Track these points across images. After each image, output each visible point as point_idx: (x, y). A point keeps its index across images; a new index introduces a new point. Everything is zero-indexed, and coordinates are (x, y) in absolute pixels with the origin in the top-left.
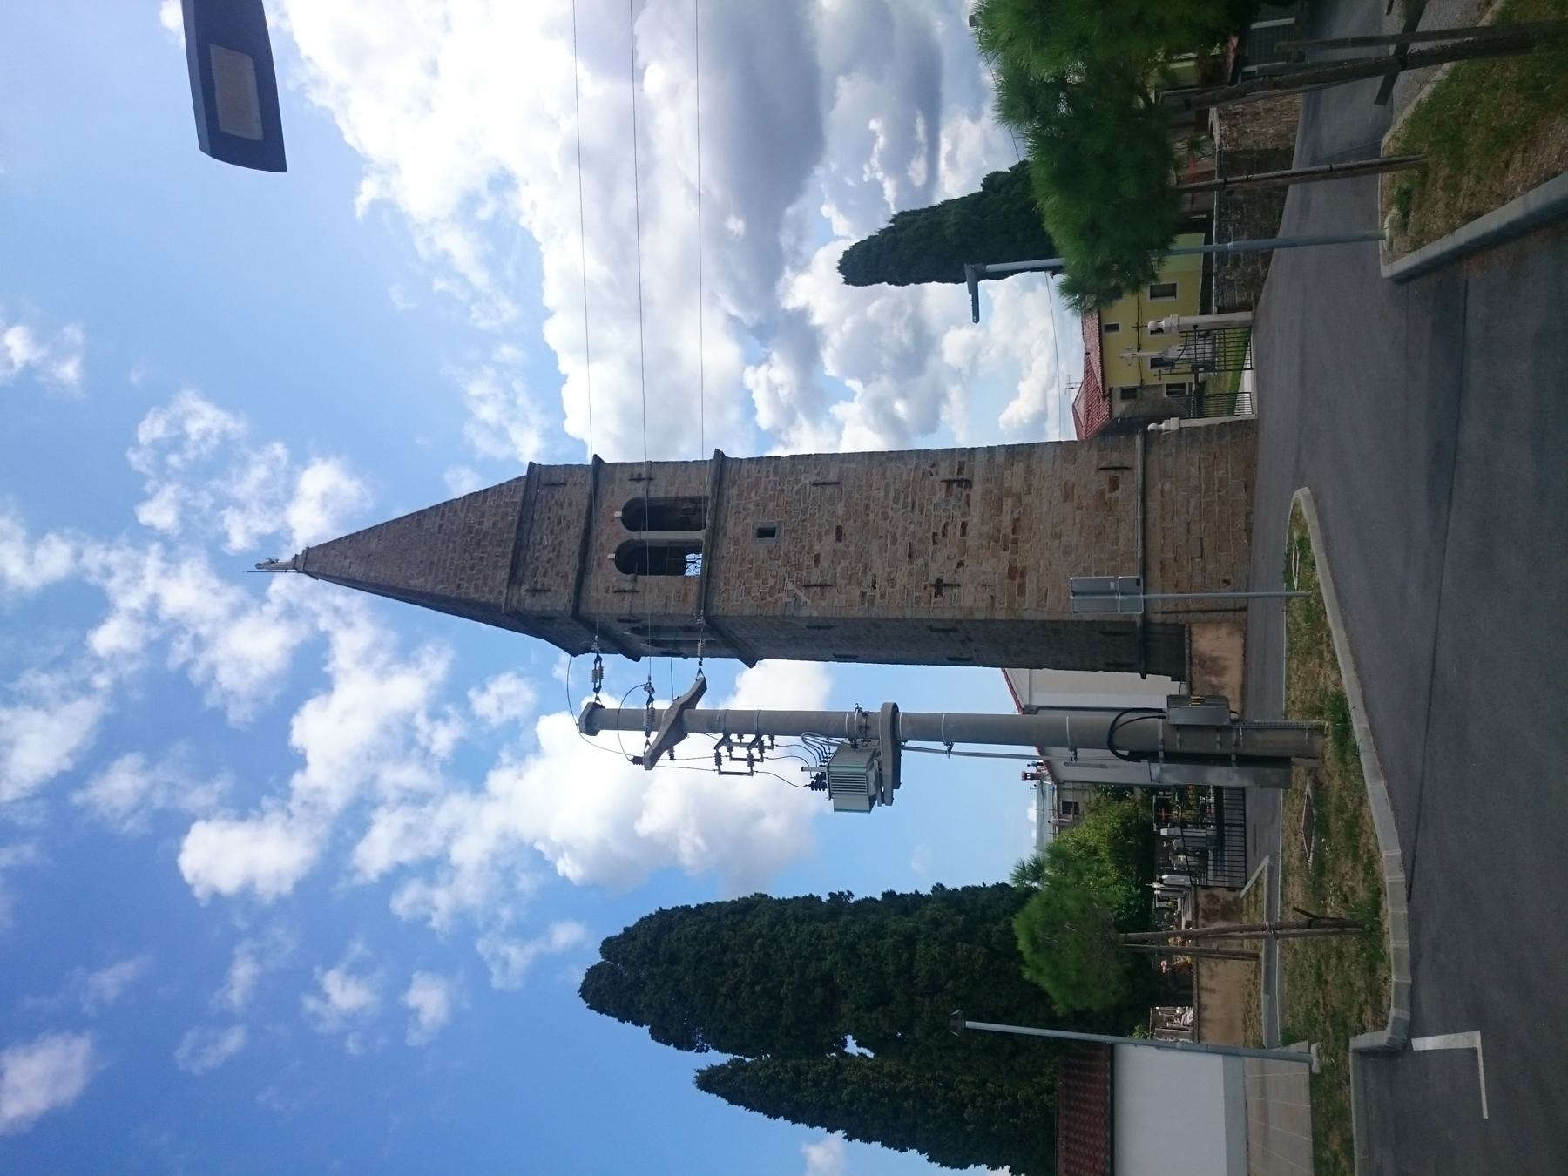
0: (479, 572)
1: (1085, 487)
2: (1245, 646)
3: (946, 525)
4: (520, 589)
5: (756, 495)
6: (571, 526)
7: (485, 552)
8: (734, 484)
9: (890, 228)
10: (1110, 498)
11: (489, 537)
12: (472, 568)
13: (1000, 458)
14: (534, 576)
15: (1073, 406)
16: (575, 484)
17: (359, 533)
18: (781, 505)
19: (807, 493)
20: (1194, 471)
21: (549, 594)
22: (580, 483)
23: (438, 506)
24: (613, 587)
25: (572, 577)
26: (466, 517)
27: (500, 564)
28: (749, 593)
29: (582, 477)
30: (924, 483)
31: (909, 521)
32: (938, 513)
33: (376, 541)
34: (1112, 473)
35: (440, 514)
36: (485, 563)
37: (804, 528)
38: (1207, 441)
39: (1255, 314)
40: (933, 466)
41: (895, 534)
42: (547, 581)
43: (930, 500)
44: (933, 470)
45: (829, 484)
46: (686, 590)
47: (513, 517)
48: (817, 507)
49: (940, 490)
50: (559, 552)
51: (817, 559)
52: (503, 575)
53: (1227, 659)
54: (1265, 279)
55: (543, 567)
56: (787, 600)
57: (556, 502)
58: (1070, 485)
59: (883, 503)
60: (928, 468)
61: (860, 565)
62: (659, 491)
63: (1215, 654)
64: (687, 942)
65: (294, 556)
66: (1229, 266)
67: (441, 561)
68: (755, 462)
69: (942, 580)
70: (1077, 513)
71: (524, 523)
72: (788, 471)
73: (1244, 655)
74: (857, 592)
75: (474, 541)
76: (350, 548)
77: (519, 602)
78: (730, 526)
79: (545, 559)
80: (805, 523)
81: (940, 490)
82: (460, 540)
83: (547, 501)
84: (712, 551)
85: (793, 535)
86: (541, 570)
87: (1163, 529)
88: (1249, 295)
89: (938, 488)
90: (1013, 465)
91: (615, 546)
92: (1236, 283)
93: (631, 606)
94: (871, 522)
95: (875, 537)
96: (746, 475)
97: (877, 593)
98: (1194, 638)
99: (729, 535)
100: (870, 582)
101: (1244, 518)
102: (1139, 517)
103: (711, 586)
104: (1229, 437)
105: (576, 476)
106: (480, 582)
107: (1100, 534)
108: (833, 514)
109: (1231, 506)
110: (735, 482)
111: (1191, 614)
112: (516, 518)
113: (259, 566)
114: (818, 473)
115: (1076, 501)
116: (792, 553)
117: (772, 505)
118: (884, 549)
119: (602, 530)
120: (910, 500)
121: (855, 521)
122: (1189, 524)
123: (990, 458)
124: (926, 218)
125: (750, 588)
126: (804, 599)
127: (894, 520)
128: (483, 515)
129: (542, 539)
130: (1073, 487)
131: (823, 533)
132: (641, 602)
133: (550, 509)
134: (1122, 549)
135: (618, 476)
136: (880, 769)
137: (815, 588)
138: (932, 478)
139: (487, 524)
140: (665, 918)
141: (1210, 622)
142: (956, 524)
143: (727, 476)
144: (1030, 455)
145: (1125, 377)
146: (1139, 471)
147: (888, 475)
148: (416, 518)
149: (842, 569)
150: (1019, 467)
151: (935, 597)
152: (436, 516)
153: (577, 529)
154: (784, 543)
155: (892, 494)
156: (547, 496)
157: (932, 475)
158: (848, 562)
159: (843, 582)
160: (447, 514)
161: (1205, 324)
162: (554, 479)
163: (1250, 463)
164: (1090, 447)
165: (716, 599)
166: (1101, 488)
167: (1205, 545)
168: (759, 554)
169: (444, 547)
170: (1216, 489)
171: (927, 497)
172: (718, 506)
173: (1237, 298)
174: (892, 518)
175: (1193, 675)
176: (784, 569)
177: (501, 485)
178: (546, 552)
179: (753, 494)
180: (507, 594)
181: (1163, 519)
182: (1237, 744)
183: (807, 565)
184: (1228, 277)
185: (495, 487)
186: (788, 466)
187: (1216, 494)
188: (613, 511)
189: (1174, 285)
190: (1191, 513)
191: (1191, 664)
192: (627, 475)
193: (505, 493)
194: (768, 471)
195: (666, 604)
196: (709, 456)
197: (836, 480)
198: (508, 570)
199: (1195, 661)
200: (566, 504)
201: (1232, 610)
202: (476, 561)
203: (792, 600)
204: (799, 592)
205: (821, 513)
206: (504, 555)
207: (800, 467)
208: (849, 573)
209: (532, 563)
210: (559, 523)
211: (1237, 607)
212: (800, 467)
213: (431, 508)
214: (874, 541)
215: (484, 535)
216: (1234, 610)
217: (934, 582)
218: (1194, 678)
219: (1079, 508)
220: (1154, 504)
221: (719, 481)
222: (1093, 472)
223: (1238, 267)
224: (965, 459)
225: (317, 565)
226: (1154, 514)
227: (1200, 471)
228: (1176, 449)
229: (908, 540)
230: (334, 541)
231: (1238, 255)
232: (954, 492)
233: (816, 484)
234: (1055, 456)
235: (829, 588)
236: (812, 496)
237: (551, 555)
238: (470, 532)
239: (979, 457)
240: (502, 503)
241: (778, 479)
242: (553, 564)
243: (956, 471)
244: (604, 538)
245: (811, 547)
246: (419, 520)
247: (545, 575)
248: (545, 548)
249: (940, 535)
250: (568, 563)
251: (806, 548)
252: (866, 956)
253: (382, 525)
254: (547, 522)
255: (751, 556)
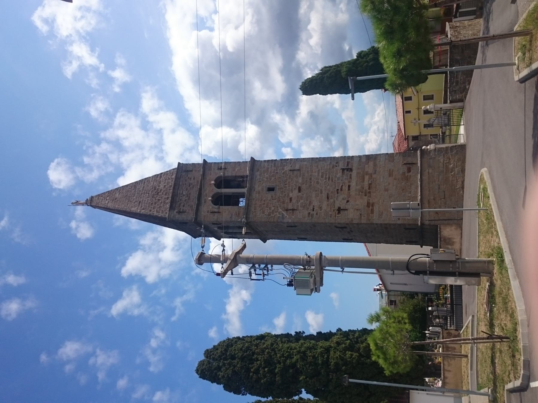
3: (342, 186)
5: (267, 175)
8: (258, 170)
9: (320, 73)
10: (408, 175)
13: (364, 160)
14: (179, 206)
15: (393, 143)
16: (196, 171)
18: (277, 178)
21: (186, 213)
24: (210, 211)
25: (195, 207)
26: (153, 184)
28: (264, 213)
31: (327, 185)
32: (339, 181)
34: (408, 166)
37: (285, 187)
40: (337, 163)
42: (185, 208)
43: (336, 176)
44: (337, 165)
45: (296, 170)
46: (239, 212)
47: (172, 183)
49: (340, 172)
50: (189, 197)
52: (168, 206)
54: (469, 89)
57: (189, 178)
60: (335, 164)
61: (308, 202)
62: (229, 173)
63: (450, 237)
64: (238, 351)
68: (266, 162)
69: (340, 208)
72: (279, 165)
74: (306, 213)
77: (173, 217)
78: (256, 187)
79: (184, 200)
83: (185, 177)
84: (249, 197)
85: (281, 190)
86: (182, 204)
89: (339, 172)
90: (368, 163)
91: (211, 195)
92: (457, 91)
93: (217, 218)
94: (312, 185)
97: (315, 213)
98: (441, 230)
100: (312, 209)
107: (404, 189)
111: (440, 221)
113: (72, 203)
116: (281, 198)
117: (273, 178)
120: (327, 176)
121: (306, 184)
124: (334, 69)
125: (265, 211)
126: (286, 215)
129: (183, 192)
130: (393, 171)
131: (293, 189)
133: (186, 180)
136: (315, 278)
138: (336, 168)
139: (162, 186)
141: (448, 224)
145: (414, 131)
147: (319, 167)
148: (134, 184)
150: (371, 163)
151: (338, 214)
155: (320, 174)
159: (301, 208)
164: (399, 155)
165: (251, 215)
171: (334, 175)
172: (252, 179)
174: (321, 184)
175: (441, 245)
177: (167, 171)
178: (184, 197)
179: (266, 174)
180: (169, 214)
182: (458, 268)
184: (454, 89)
185: (165, 172)
186: (280, 163)
188: (211, 181)
189: (433, 95)
190: (440, 181)
195: (231, 217)
197: (298, 169)
199: (442, 239)
200: (192, 179)
203: (281, 216)
204: (284, 212)
207: (284, 164)
209: (179, 201)
210: (190, 185)
212: (284, 164)
217: (337, 208)
219: (395, 179)
220: (425, 178)
221: (252, 169)
222: (401, 165)
224: (350, 160)
227: (443, 165)
232: (345, 174)
234: (385, 159)
236: (289, 175)
237: (187, 198)
238: (155, 190)
241: (276, 168)
242: (187, 202)
245: (288, 195)
247: (184, 206)
248: (184, 195)
249: (340, 190)
250: (193, 201)
251: (287, 195)
252: (310, 356)
254: (185, 185)
255: (265, 199)
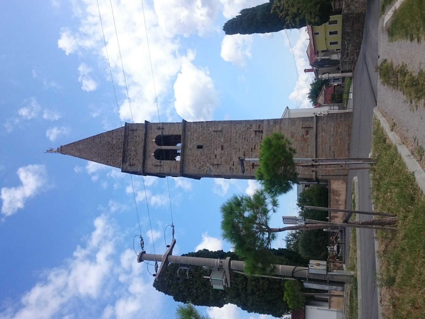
0: (113, 157)
1: (298, 134)
2: (347, 187)
3: (255, 145)
4: (126, 164)
5: (196, 134)
6: (140, 144)
7: (114, 151)
8: (189, 131)
10: (306, 137)
11: (115, 146)
12: (111, 156)
13: (272, 123)
14: (130, 160)
16: (140, 130)
17: (76, 142)
18: (204, 138)
19: (212, 134)
20: (332, 129)
21: (135, 166)
22: (142, 130)
23: (99, 135)
24: (154, 164)
25: (141, 161)
26: (108, 139)
27: (119, 155)
28: (196, 166)
29: (142, 128)
30: (248, 131)
31: (244, 144)
32: (253, 141)
33: (81, 145)
34: (306, 129)
35: (100, 137)
36: (115, 155)
37: (211, 146)
38: (336, 119)
39: (353, 74)
40: (251, 126)
41: (239, 148)
42: (134, 162)
43: (250, 137)
44: (251, 127)
45: (219, 131)
46: (176, 165)
47: (122, 140)
48: (215, 139)
49: (253, 134)
50: (137, 152)
51: (216, 156)
52: (121, 159)
53: (341, 191)
54: (357, 61)
55: (132, 157)
56: (207, 169)
57: (135, 136)
58: (293, 133)
59: (235, 138)
60: (249, 126)
61: (229, 158)
62: (166, 133)
63: (337, 190)
64: (182, 275)
65: (57, 148)
66: (345, 56)
67: (102, 154)
68: (195, 123)
69: (254, 164)
70: (295, 142)
71: (126, 143)
72: (205, 126)
73: (346, 190)
74: (228, 167)
75: (111, 147)
76: (74, 147)
77: (126, 168)
78: (188, 144)
79: (133, 154)
80: (212, 144)
81: (253, 134)
82: (106, 147)
83: (132, 135)
84: (183, 153)
85: (208, 148)
86: (132, 158)
87: (322, 148)
88: (351, 67)
89: (252, 133)
90: (275, 126)
91: (154, 151)
92: (347, 62)
93: (160, 171)
94: (232, 144)
95: (233, 149)
96: (193, 128)
97: (234, 167)
98: (331, 184)
99: (189, 147)
100: (232, 164)
101: (347, 145)
102: (315, 145)
103: (184, 165)
104: (344, 118)
105: (140, 127)
106: (114, 161)
107: (303, 149)
108: (220, 141)
109: (344, 141)
110: (189, 130)
111: (330, 176)
112: (123, 140)
113: (47, 151)
114: (215, 128)
115: (295, 138)
116: (208, 154)
117: (201, 138)
118: (236, 153)
119: (149, 145)
120: (244, 137)
121: (227, 143)
122: (330, 147)
123: (268, 123)
125: (196, 165)
126: (212, 169)
127: (239, 143)
128: (113, 139)
129: (131, 148)
130: (294, 134)
131: (217, 147)
132: (163, 169)
133: (133, 138)
134: (309, 154)
135: (153, 127)
137: (216, 165)
138: (250, 129)
139: (114, 142)
140: (176, 265)
141: (336, 179)
142: (258, 145)
143: (187, 128)
144: (281, 123)
146: (315, 129)
147: (237, 128)
148: (93, 138)
149: (224, 159)
150: (278, 126)
151: (252, 169)
152: (99, 138)
153: (142, 145)
154: (206, 150)
155: (238, 135)
156: (132, 134)
157: (250, 128)
158: (225, 157)
159: (224, 164)
160: (102, 138)
161: (336, 77)
162: (134, 128)
163: (350, 127)
164: (299, 120)
165: (186, 168)
166: (303, 134)
167: (335, 154)
168: (198, 154)
169: (102, 148)
170: (339, 135)
171: (249, 136)
172: (184, 138)
173: (347, 68)
174: (238, 143)
175: (331, 196)
176: (206, 159)
177: (117, 129)
178: (133, 152)
179: (195, 134)
180: (122, 166)
181: (322, 145)
183: (213, 158)
184: (345, 60)
185: (116, 129)
186: (206, 125)
187: (339, 137)
188: (152, 139)
190: (331, 143)
191: (330, 193)
192: (156, 128)
193: (119, 132)
194: (200, 127)
195: (170, 170)
196: (181, 121)
197: (221, 130)
198: (122, 157)
199: (331, 192)
200: (138, 137)
201: (343, 175)
202: (112, 154)
203: (208, 169)
204: (211, 166)
205: (216, 141)
206: (120, 152)
207: (209, 125)
208: (226, 161)
209: (129, 156)
210: (136, 143)
211: (345, 174)
212: (209, 125)
213: (97, 135)
214: (233, 150)
215: (114, 145)
216: (344, 176)
217: (252, 164)
218: (331, 197)
219: (296, 140)
220: (319, 140)
221: (184, 130)
222: (300, 129)
223: (348, 56)
224: (261, 123)
225: (65, 152)
226: (319, 143)
227: (334, 129)
228: (327, 121)
229: (244, 150)
230: (69, 144)
231: (348, 52)
232: (257, 135)
233: (214, 131)
234: (289, 123)
235: (220, 165)
236: (213, 135)
237: (135, 153)
238: (109, 144)
239: (265, 123)
240: (118, 135)
241: (203, 129)
242: (135, 156)
243: (258, 127)
244: (150, 148)
245: (214, 152)
246: (93, 139)
247: (133, 160)
248: (132, 151)
249: (253, 148)
250: (140, 156)
251: (212, 152)
252: (233, 283)
253: (83, 140)
254: (132, 142)
255: (196, 155)
